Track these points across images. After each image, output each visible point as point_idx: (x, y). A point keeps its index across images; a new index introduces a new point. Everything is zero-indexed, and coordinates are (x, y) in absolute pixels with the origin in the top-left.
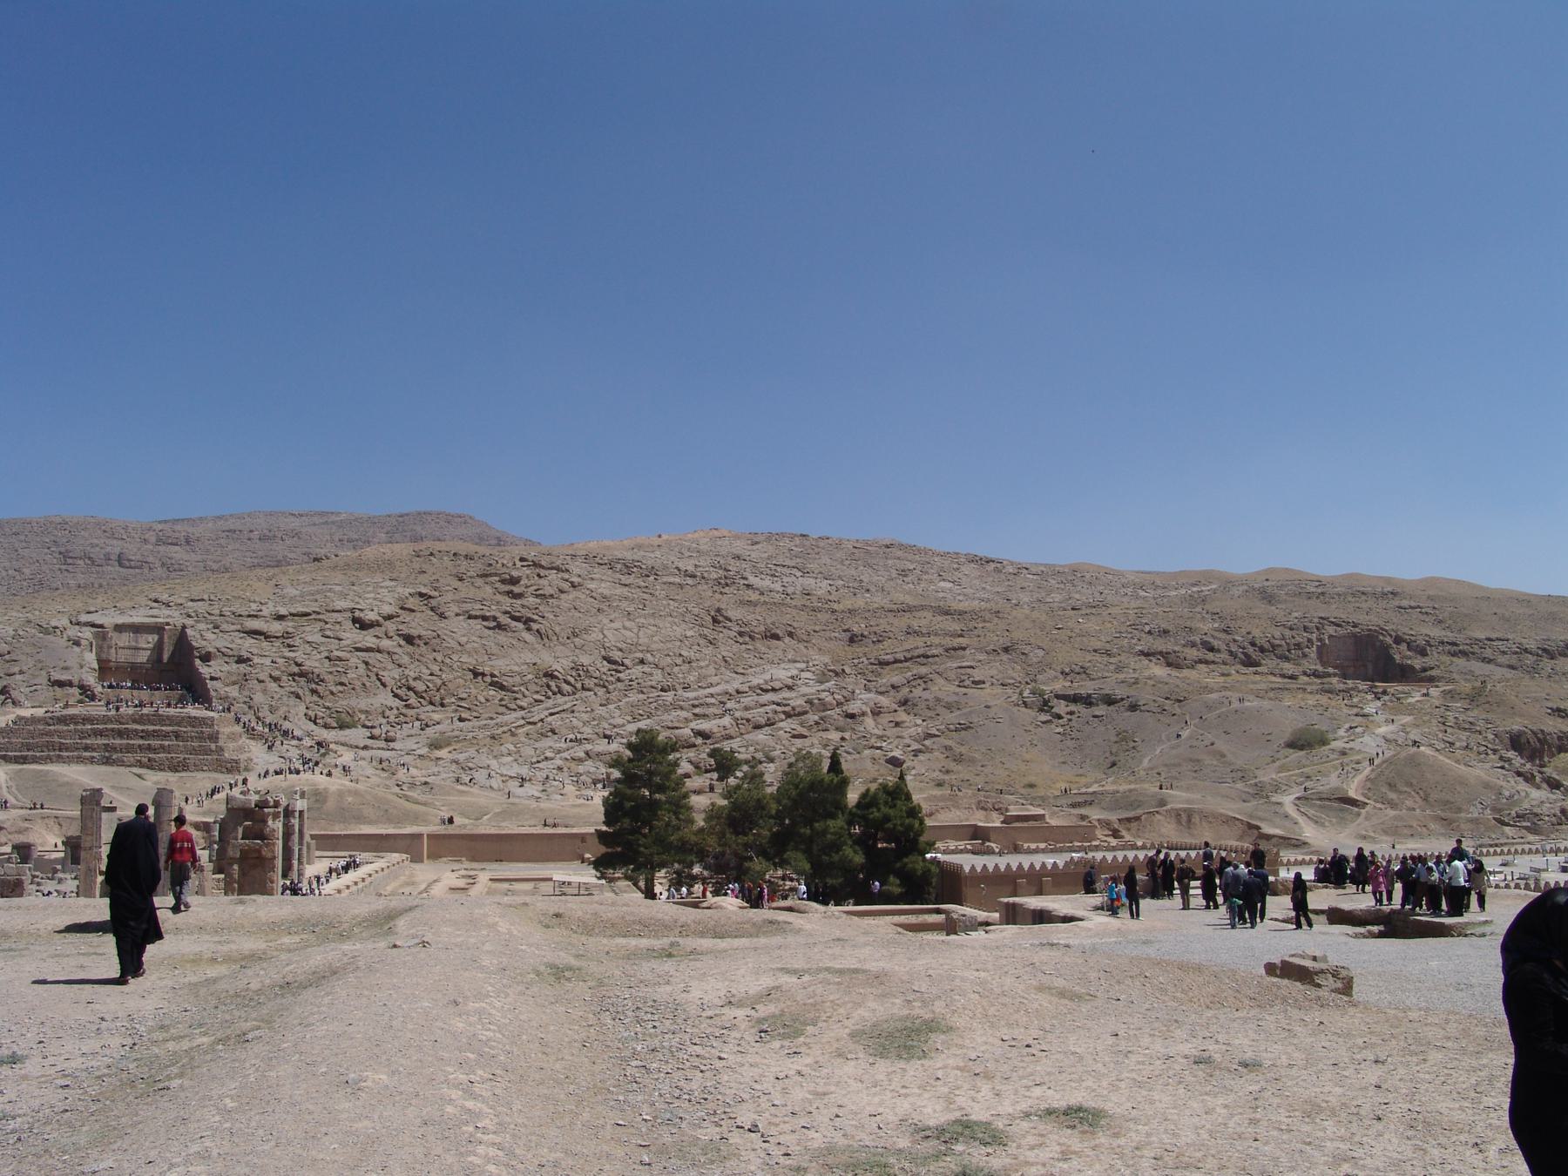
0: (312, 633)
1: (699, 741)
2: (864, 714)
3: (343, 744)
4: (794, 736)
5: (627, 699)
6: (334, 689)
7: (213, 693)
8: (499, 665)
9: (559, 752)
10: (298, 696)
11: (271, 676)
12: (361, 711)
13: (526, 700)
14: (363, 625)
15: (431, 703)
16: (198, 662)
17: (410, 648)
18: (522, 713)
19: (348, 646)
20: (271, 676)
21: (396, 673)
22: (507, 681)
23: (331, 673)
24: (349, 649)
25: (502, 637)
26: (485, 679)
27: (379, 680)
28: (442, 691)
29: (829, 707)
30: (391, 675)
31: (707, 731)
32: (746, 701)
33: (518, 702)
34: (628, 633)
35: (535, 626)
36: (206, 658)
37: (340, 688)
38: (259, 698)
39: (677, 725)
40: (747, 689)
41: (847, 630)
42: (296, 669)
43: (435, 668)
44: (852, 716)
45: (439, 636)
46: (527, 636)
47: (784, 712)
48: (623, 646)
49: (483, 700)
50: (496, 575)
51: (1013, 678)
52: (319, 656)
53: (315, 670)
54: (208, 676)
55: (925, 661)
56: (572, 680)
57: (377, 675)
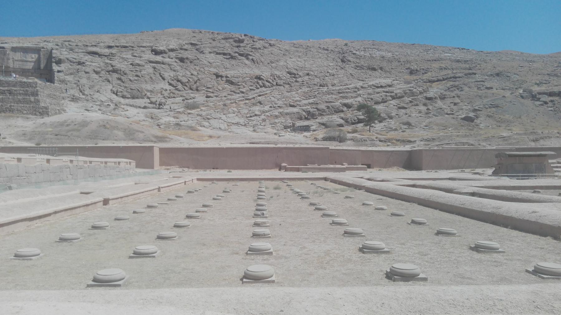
0: (128, 55)
1: (345, 109)
2: (436, 98)
3: (131, 106)
4: (400, 108)
5: (301, 90)
6: (131, 78)
7: (56, 78)
8: (230, 73)
9: (264, 112)
10: (109, 81)
11: (94, 71)
12: (148, 91)
13: (244, 89)
14: (156, 52)
15: (191, 89)
16: (54, 64)
17: (181, 64)
18: (243, 95)
19: (145, 60)
20: (94, 71)
21: (172, 74)
22: (235, 80)
23: (132, 71)
24: (146, 61)
25: (233, 62)
26: (223, 79)
27: (161, 76)
28: (198, 84)
29: (415, 94)
30: (169, 74)
31: (350, 104)
32: (370, 91)
33: (241, 89)
34: (299, 63)
35: (251, 57)
36: (59, 62)
37: (136, 78)
38: (84, 81)
39: (332, 101)
40: (367, 86)
41: (409, 68)
42: (111, 69)
43: (195, 73)
44: (430, 99)
45: (198, 59)
46: (247, 62)
47: (391, 96)
48: (298, 68)
49: (221, 89)
50: (231, 38)
51: (508, 87)
52: (127, 63)
53: (122, 69)
54: (56, 70)
55: (455, 80)
56: (271, 81)
57: (160, 74)
